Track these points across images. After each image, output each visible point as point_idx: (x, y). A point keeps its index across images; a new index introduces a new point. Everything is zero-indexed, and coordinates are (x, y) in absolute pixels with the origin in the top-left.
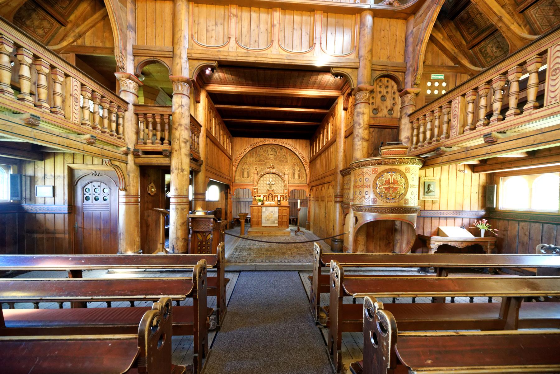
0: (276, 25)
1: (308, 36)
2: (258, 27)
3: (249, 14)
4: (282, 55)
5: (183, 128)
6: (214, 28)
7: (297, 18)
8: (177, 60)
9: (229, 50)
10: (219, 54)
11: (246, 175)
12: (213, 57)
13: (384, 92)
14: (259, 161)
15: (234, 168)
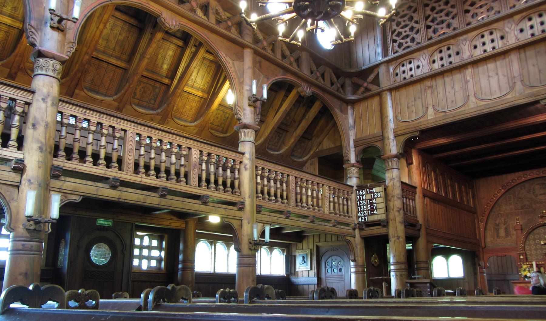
0: (469, 81)
1: (506, 78)
3: (443, 80)
4: (480, 106)
5: (395, 198)
6: (413, 103)
8: (386, 142)
9: (428, 118)
10: (420, 124)
11: (502, 233)
12: (415, 129)
14: (522, 208)
15: (482, 225)
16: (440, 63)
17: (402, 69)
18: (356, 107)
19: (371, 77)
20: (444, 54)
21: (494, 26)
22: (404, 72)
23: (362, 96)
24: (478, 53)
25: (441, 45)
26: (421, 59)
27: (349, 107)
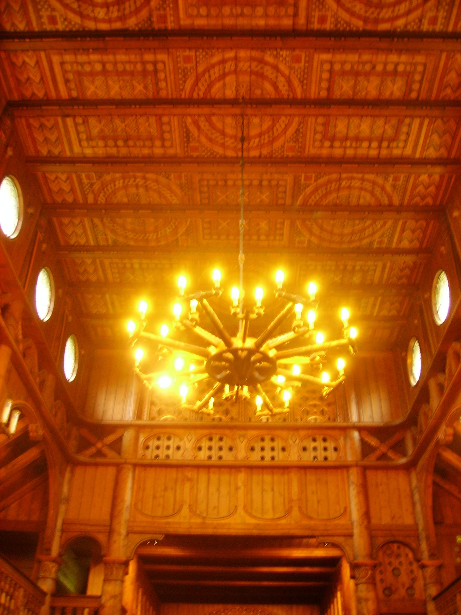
2: (218, 490)
7: (268, 478)
13: (395, 563)
16: (208, 453)
17: (157, 443)
18: (79, 471)
19: (110, 439)
20: (215, 444)
21: (278, 432)
22: (158, 448)
23: (93, 460)
24: (255, 458)
25: (214, 431)
26: (185, 439)
27: (69, 469)
